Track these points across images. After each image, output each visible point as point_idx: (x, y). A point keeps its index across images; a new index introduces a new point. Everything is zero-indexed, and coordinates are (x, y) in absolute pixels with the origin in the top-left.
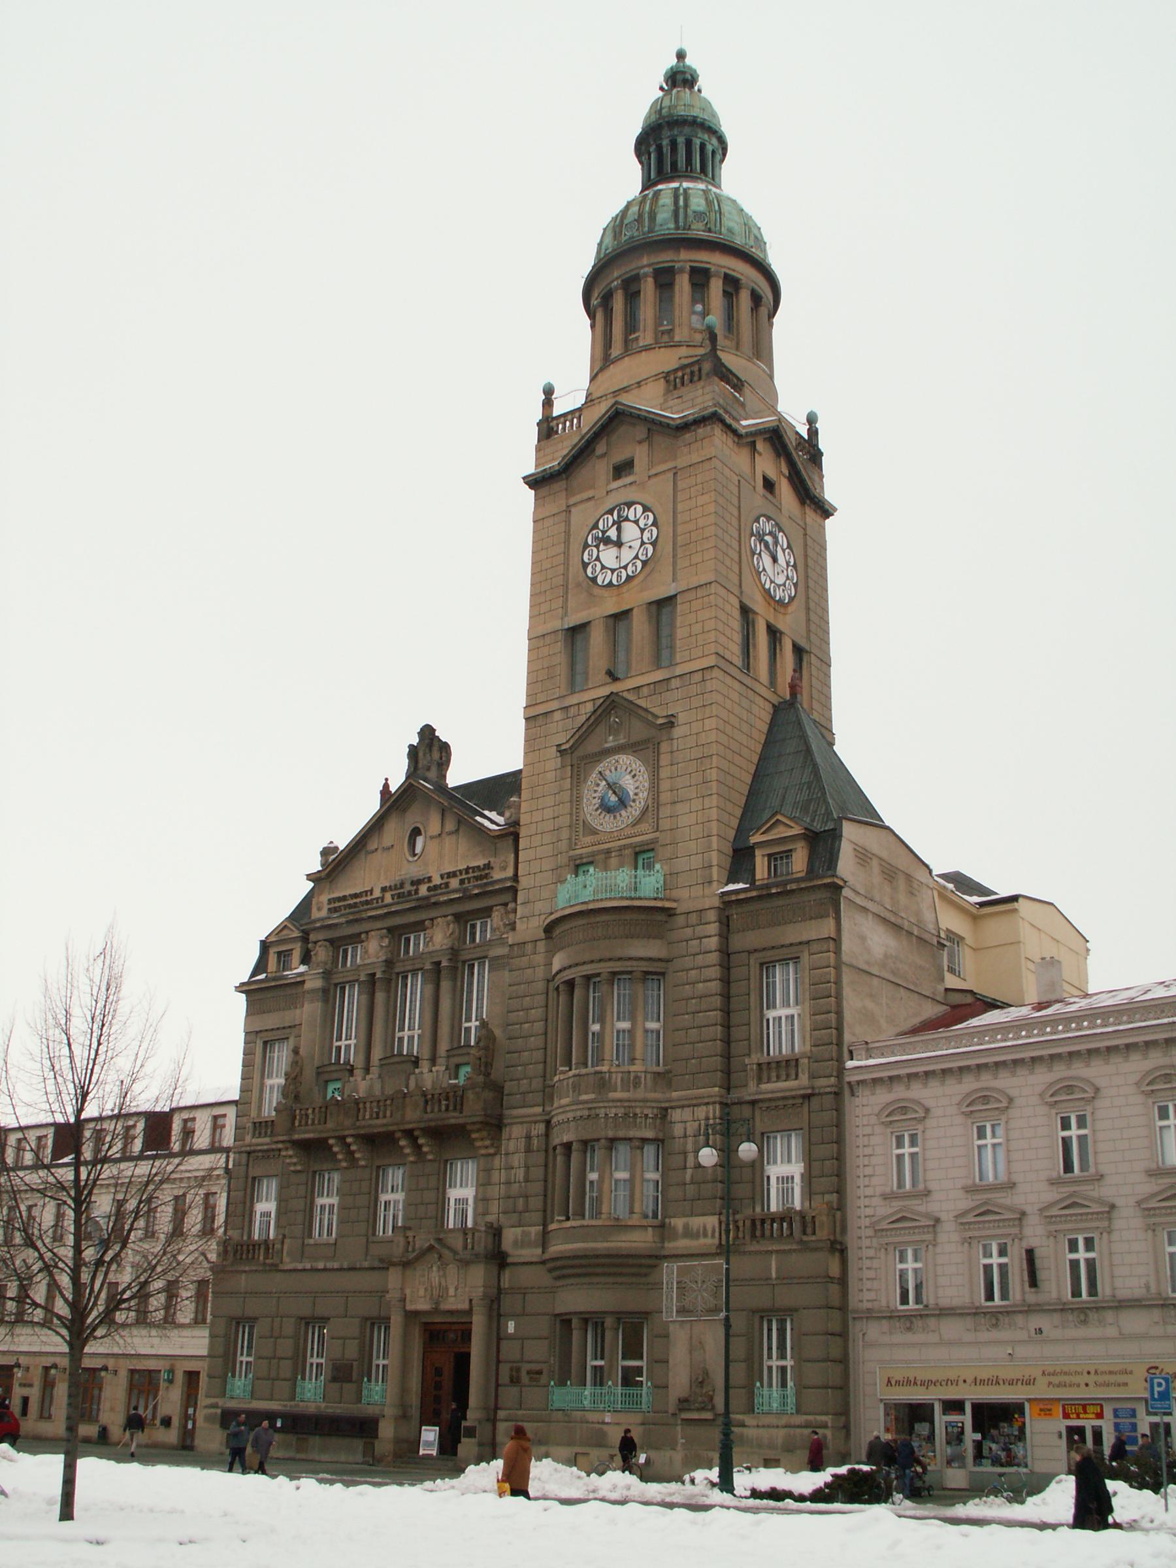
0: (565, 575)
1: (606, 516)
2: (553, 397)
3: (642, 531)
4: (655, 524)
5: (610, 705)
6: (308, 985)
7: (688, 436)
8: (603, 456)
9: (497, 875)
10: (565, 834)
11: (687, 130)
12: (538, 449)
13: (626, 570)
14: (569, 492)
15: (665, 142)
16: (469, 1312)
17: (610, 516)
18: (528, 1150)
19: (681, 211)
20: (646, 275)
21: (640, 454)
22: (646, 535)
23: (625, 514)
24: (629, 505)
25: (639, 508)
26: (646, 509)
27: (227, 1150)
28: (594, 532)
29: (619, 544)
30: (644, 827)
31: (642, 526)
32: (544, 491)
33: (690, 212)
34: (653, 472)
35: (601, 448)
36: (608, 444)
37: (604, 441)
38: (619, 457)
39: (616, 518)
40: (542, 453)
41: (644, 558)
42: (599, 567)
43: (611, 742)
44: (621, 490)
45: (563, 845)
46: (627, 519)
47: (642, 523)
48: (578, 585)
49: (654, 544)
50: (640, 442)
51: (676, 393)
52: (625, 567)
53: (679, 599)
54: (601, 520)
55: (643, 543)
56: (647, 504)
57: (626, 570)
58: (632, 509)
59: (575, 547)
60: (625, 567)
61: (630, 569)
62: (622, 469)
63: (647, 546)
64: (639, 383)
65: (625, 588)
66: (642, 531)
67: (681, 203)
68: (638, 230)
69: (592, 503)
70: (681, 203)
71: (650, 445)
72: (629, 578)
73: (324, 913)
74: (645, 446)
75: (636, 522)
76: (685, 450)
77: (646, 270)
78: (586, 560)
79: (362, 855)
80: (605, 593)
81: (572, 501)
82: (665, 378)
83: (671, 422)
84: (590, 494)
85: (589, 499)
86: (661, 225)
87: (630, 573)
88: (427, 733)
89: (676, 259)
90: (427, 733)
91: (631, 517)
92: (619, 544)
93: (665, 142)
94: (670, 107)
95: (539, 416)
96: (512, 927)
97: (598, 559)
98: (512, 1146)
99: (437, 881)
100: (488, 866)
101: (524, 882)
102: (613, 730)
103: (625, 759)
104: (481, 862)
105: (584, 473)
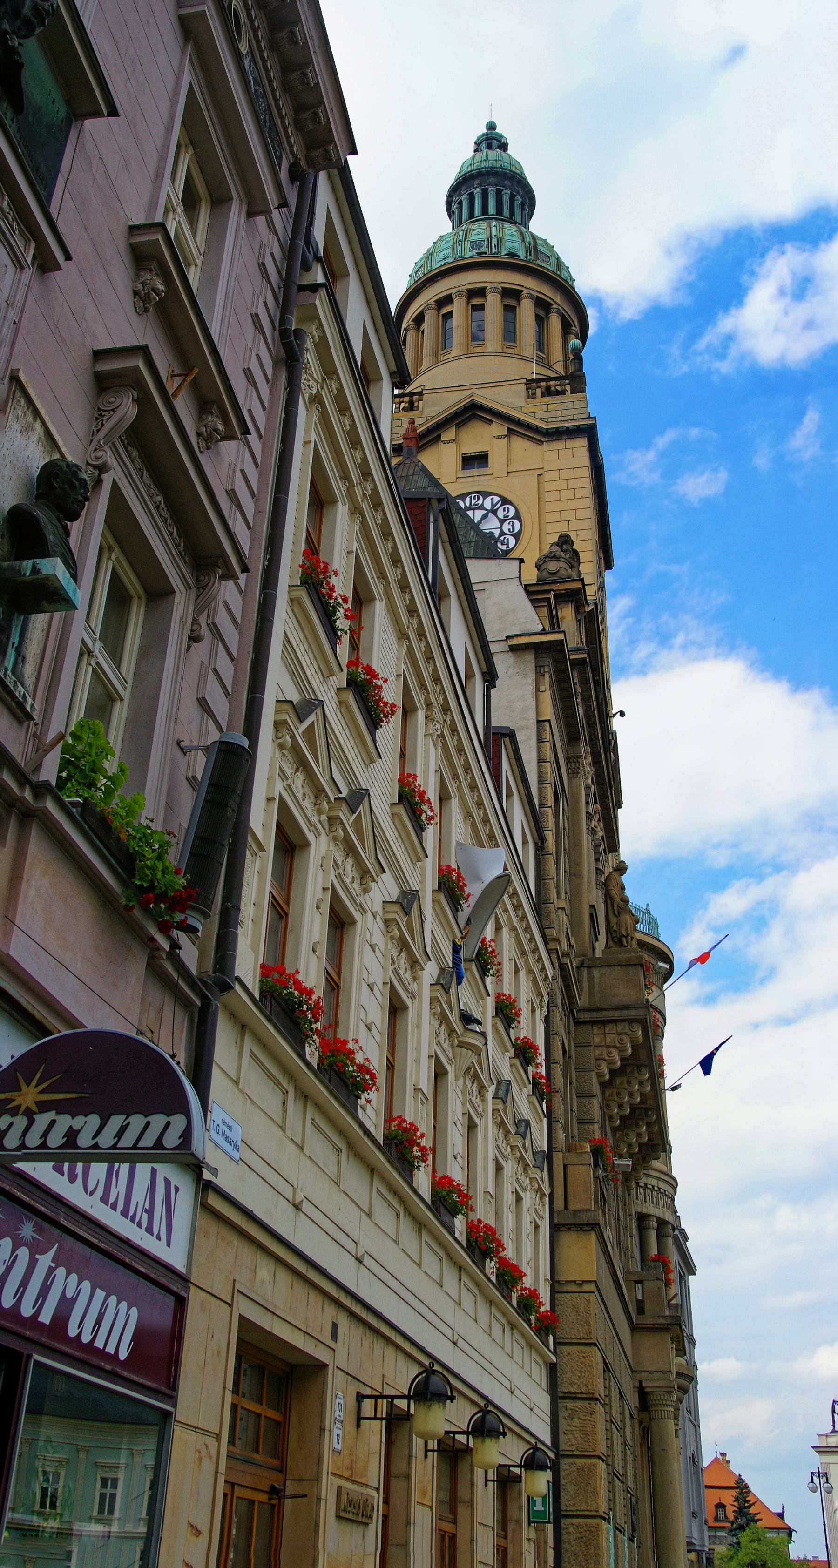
3: (502, 522)
4: (517, 516)
8: (450, 442)
21: (497, 451)
22: (506, 527)
23: (480, 502)
24: (486, 495)
35: (449, 434)
36: (457, 435)
38: (471, 447)
47: (501, 514)
49: (517, 536)
50: (498, 437)
55: (502, 533)
58: (488, 500)
63: (507, 537)
66: (502, 522)
82: (526, 384)
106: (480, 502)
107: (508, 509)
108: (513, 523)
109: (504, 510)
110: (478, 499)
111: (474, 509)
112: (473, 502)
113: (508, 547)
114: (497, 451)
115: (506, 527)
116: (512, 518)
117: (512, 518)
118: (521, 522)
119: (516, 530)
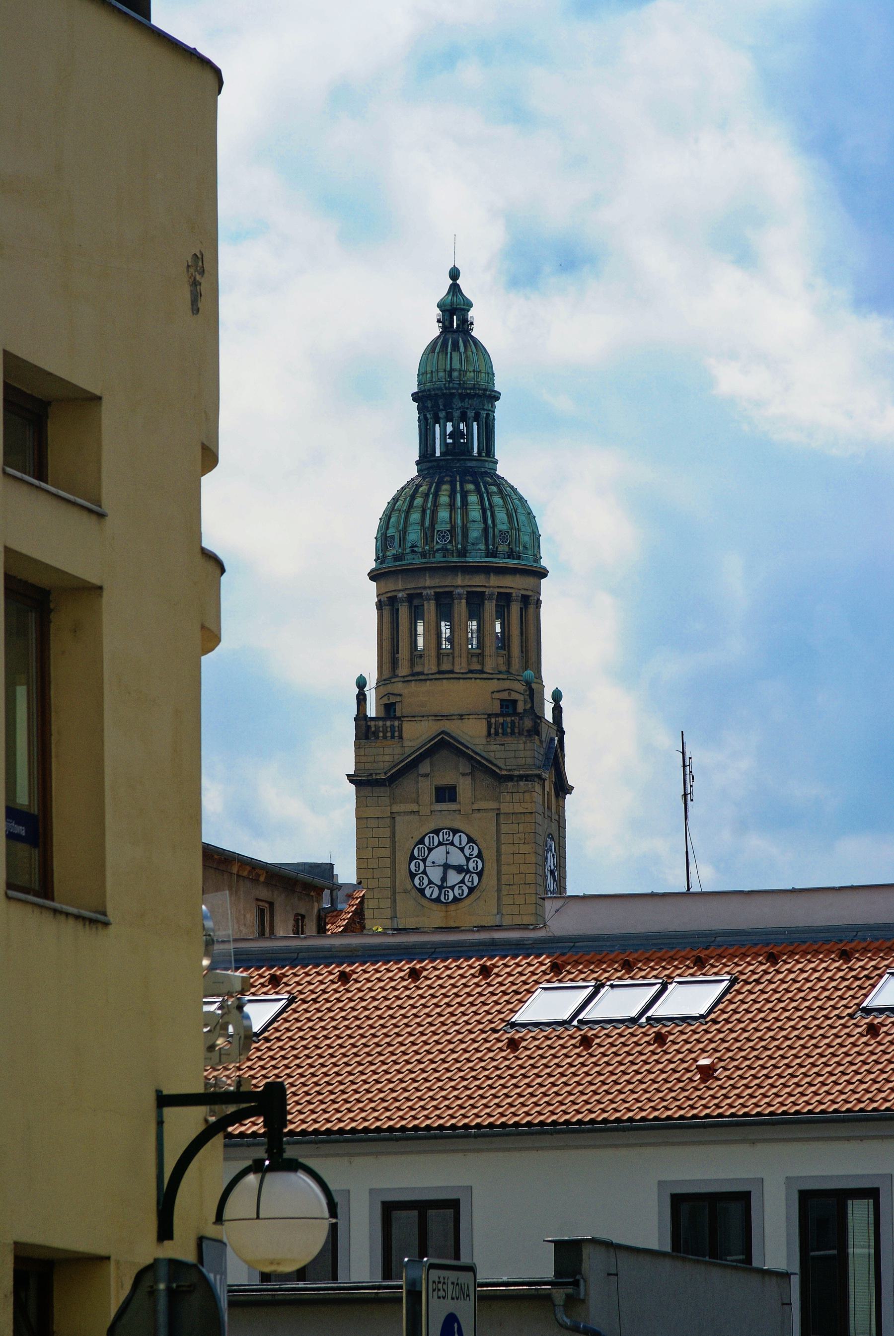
0: (394, 882)
1: (431, 835)
2: (365, 690)
3: (468, 859)
4: (480, 856)
7: (510, 784)
8: (426, 775)
11: (475, 402)
12: (358, 746)
13: (453, 890)
14: (393, 800)
17: (436, 837)
19: (490, 530)
20: (460, 596)
21: (465, 788)
24: (455, 831)
25: (465, 839)
26: (470, 840)
28: (421, 846)
29: (446, 867)
31: (468, 856)
32: (367, 790)
33: (497, 531)
34: (476, 807)
35: (425, 768)
37: (427, 761)
39: (441, 840)
40: (362, 752)
41: (470, 884)
42: (426, 881)
46: (452, 844)
47: (467, 852)
48: (406, 892)
50: (463, 775)
51: (499, 740)
52: (452, 888)
54: (427, 838)
56: (472, 836)
57: (453, 890)
59: (402, 857)
60: (452, 888)
62: (446, 794)
64: (461, 716)
65: (452, 907)
67: (490, 522)
68: (450, 542)
69: (415, 818)
70: (490, 522)
71: (473, 780)
72: (455, 900)
74: (469, 778)
75: (462, 849)
76: (508, 797)
77: (460, 590)
78: (413, 870)
80: (434, 906)
81: (396, 808)
82: (486, 719)
83: (497, 771)
84: (415, 808)
85: (413, 812)
86: (473, 544)
87: (457, 895)
89: (487, 585)
91: (457, 842)
92: (446, 867)
94: (460, 370)
95: (354, 712)
97: (424, 872)
105: (407, 785)
106: (451, 838)
107: (473, 846)
108: (477, 862)
109: (470, 848)
110: (449, 836)
111: (446, 844)
112: (445, 837)
113: (473, 884)
114: (465, 788)
115: (471, 865)
116: (475, 857)
117: (475, 857)
118: (482, 861)
119: (480, 868)
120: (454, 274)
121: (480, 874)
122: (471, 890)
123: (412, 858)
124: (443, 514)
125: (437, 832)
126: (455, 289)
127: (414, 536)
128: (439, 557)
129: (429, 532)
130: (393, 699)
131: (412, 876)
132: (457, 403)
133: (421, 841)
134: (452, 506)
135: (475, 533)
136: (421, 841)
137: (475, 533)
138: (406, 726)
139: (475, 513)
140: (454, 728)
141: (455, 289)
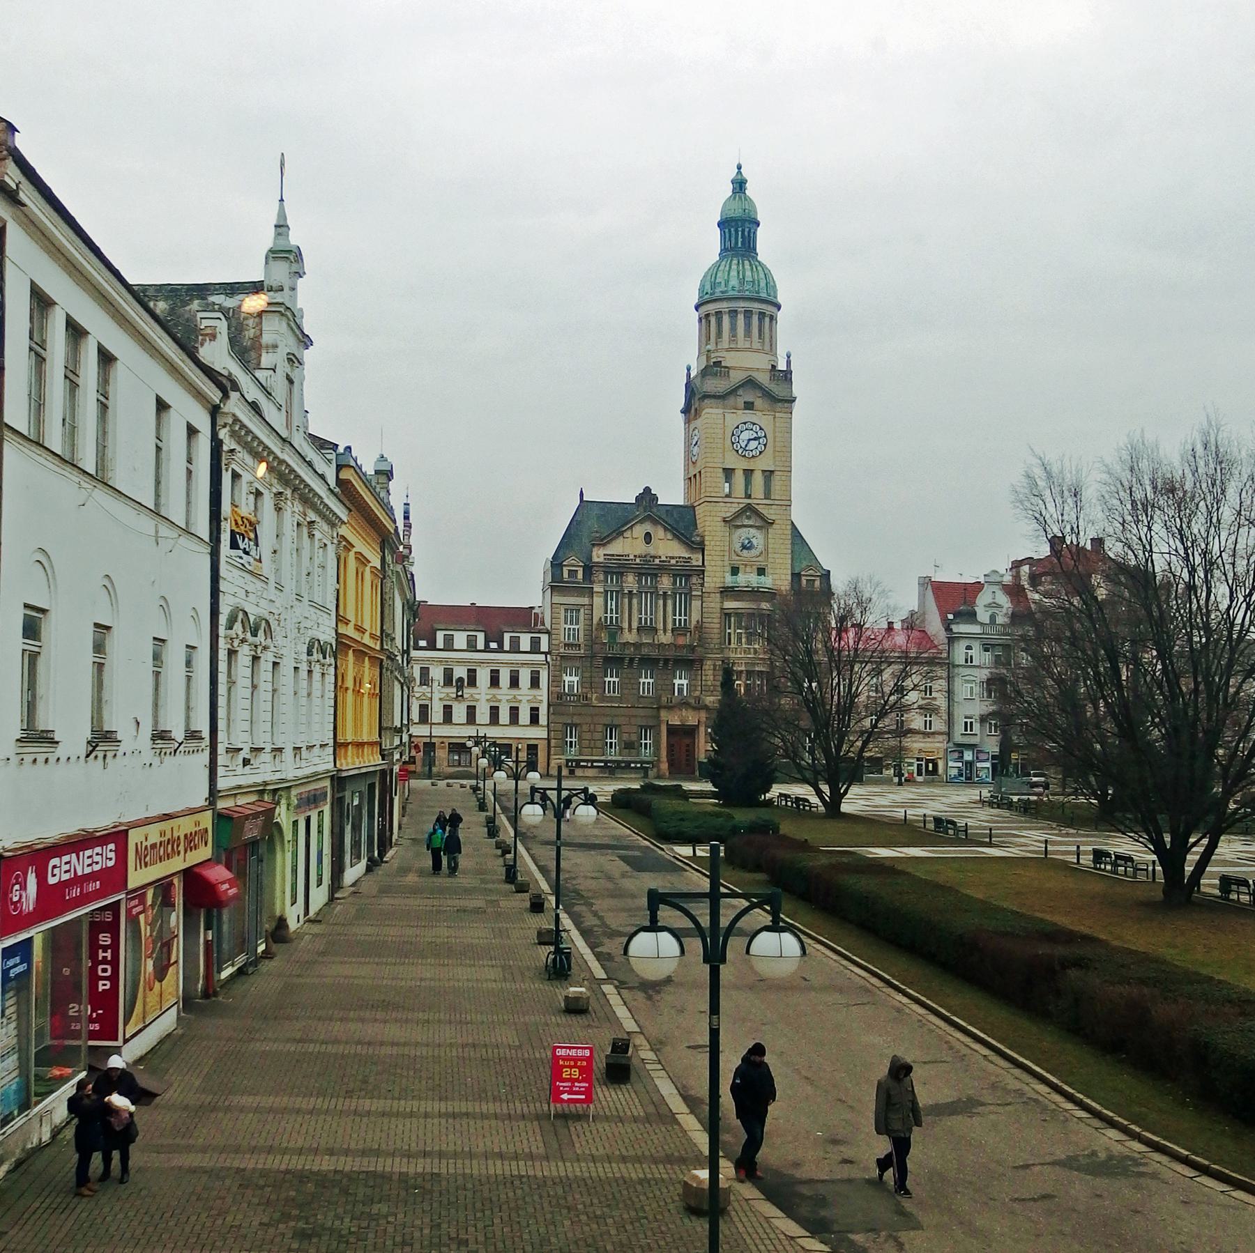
5: (749, 507)
6: (595, 590)
9: (695, 563)
10: (727, 554)
15: (747, 230)
16: (698, 726)
18: (714, 670)
21: (759, 403)
24: (754, 424)
26: (761, 429)
27: (546, 654)
30: (760, 559)
35: (740, 392)
43: (746, 522)
44: (749, 416)
45: (726, 558)
49: (765, 445)
53: (776, 473)
61: (754, 453)
62: (749, 406)
73: (601, 560)
79: (621, 538)
88: (647, 490)
90: (647, 490)
93: (747, 230)
96: (702, 585)
98: (707, 667)
99: (663, 558)
100: (689, 558)
101: (708, 568)
102: (749, 518)
103: (753, 531)
104: (687, 556)
105: (731, 401)
120: (739, 167)
121: (765, 445)
122: (760, 453)
123: (733, 435)
124: (748, 273)
125: (745, 423)
126: (739, 172)
127: (734, 282)
128: (747, 293)
129: (742, 281)
130: (719, 359)
131: (733, 443)
132: (747, 225)
133: (737, 427)
134: (752, 269)
135: (763, 284)
136: (737, 427)
137: (763, 284)
138: (731, 371)
139: (762, 276)
140: (755, 374)
141: (739, 172)
